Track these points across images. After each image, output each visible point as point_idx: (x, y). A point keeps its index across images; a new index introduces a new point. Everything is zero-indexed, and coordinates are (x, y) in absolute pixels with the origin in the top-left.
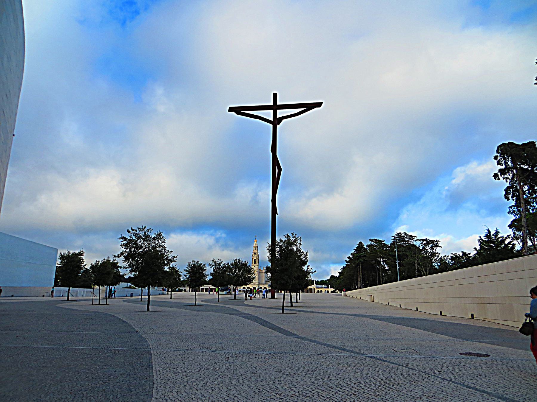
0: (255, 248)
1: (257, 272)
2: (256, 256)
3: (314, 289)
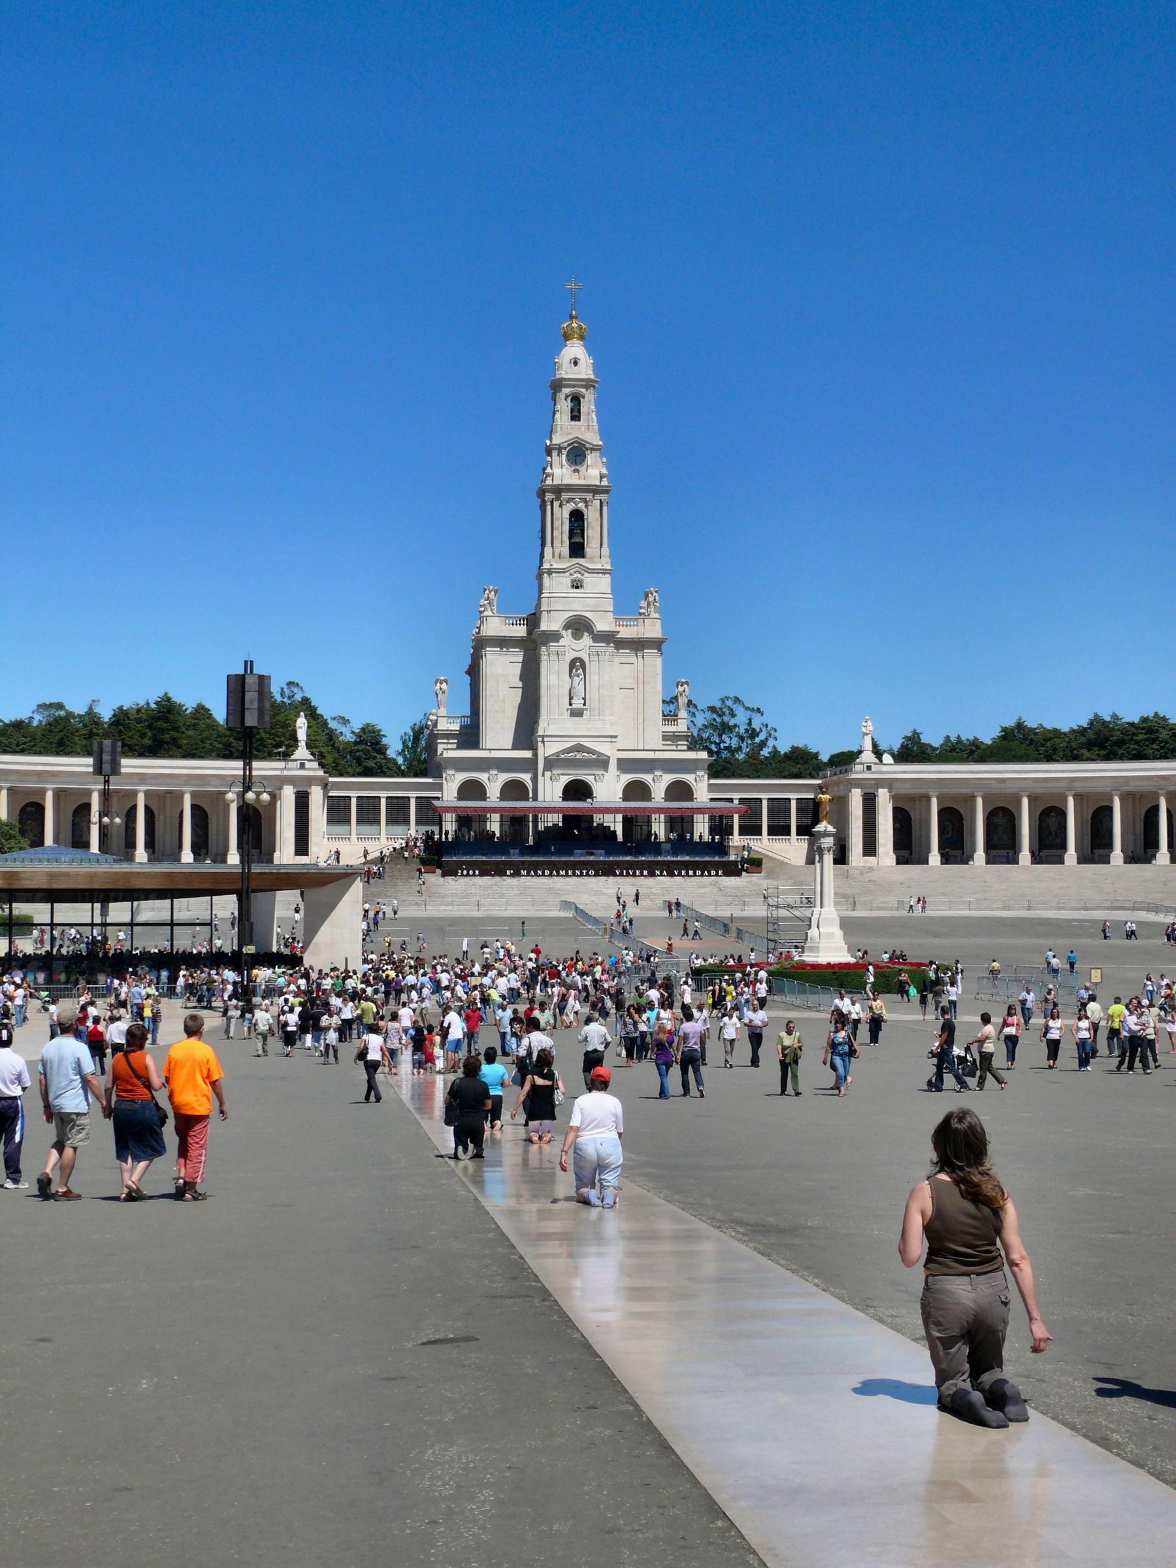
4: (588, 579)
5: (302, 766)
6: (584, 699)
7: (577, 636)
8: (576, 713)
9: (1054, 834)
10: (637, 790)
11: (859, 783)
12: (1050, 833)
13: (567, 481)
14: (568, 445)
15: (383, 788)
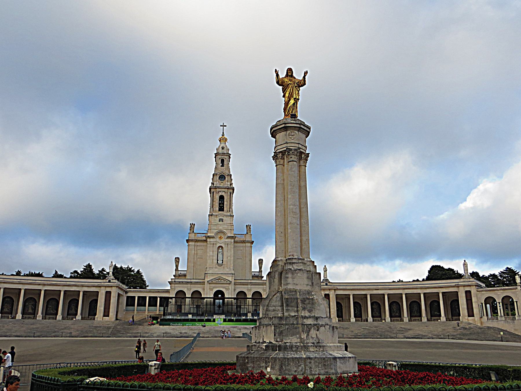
0: (223, 161)
1: (229, 237)
3: (468, 294)
4: (224, 218)
5: (109, 282)
6: (223, 261)
8: (220, 265)
9: (395, 311)
10: (242, 295)
11: (324, 290)
12: (394, 311)
14: (220, 174)
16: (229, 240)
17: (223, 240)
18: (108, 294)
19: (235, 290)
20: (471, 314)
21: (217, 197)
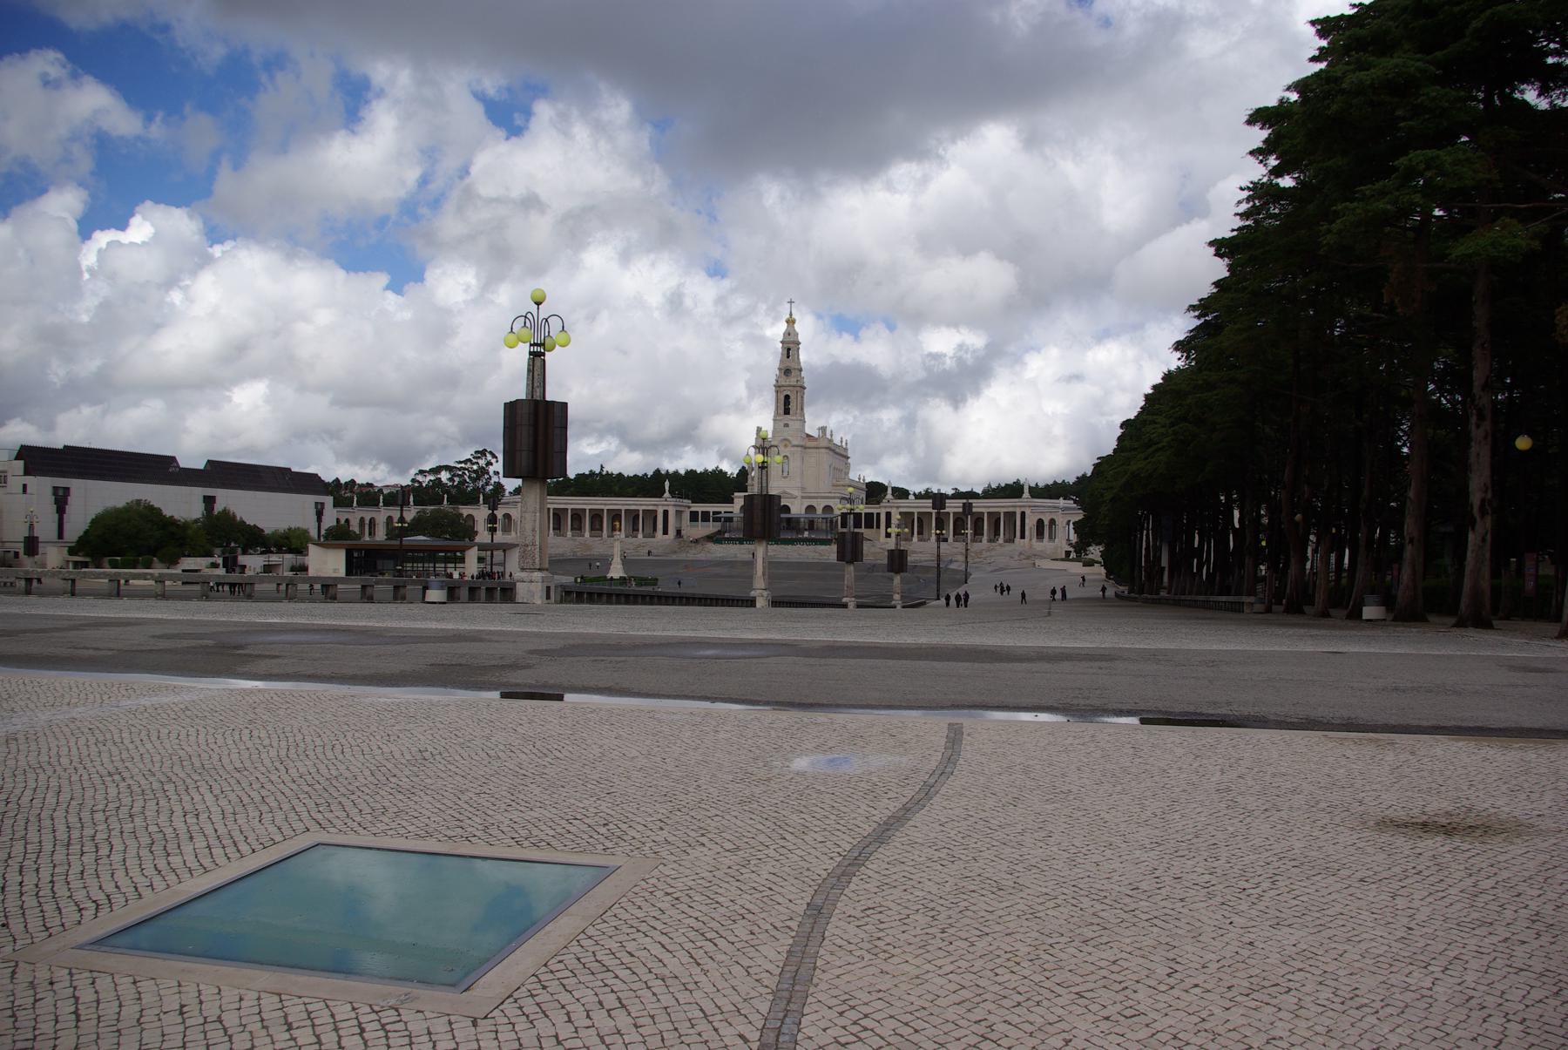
0: (789, 349)
2: (792, 381)
3: (1023, 514)
4: (790, 423)
5: (666, 500)
7: (786, 446)
8: (786, 477)
10: (810, 509)
11: (885, 507)
13: (783, 383)
15: (711, 508)
16: (795, 448)
17: (787, 449)
18: (666, 513)
19: (802, 504)
20: (1023, 536)
21: (782, 398)
